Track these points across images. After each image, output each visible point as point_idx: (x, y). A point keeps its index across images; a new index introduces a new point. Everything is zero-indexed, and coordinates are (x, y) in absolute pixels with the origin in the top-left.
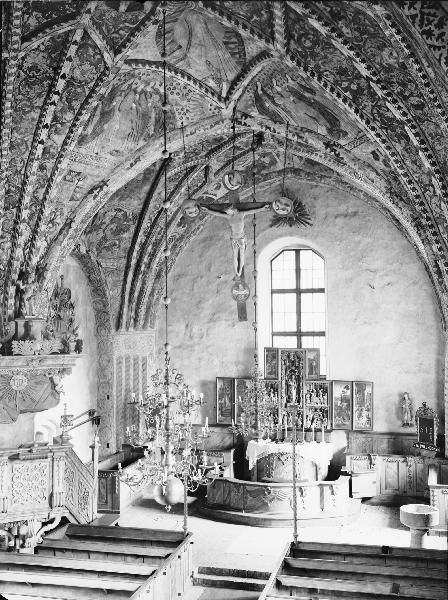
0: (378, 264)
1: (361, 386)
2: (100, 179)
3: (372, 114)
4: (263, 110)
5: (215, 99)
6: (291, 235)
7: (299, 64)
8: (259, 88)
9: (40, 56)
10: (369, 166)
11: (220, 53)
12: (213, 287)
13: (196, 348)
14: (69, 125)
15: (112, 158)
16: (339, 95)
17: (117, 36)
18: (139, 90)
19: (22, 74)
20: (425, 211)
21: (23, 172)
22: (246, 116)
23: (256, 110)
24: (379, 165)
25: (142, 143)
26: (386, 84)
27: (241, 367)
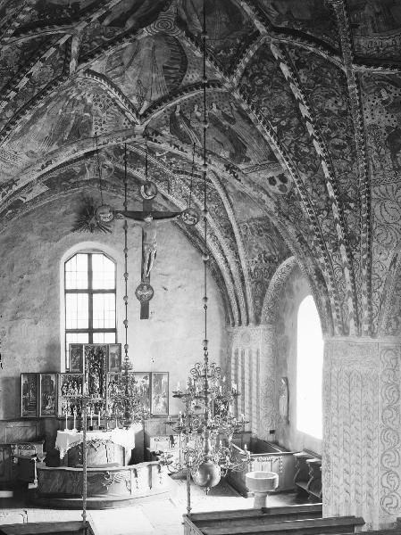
0: (171, 269)
1: (159, 376)
2: (10, 178)
3: (289, 147)
4: (175, 130)
5: (134, 115)
6: (92, 239)
7: (244, 98)
8: (178, 111)
10: (262, 188)
11: (154, 76)
12: (16, 286)
15: (27, 158)
16: (268, 128)
17: (88, 46)
18: (71, 97)
20: (317, 230)
22: (157, 133)
23: (168, 129)
24: (275, 189)
25: (55, 147)
26: (318, 126)
27: (43, 363)
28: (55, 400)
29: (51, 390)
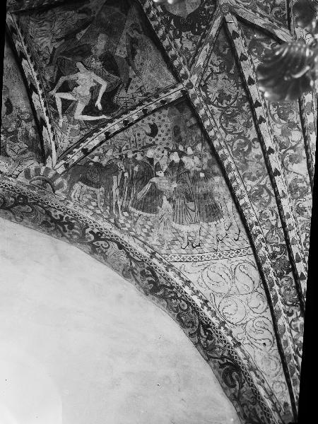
9: (220, 80)
14: (302, 144)
19: (216, 109)
21: (280, 225)
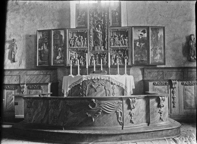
13: (21, 11)
28: (64, 52)
29: (62, 46)
